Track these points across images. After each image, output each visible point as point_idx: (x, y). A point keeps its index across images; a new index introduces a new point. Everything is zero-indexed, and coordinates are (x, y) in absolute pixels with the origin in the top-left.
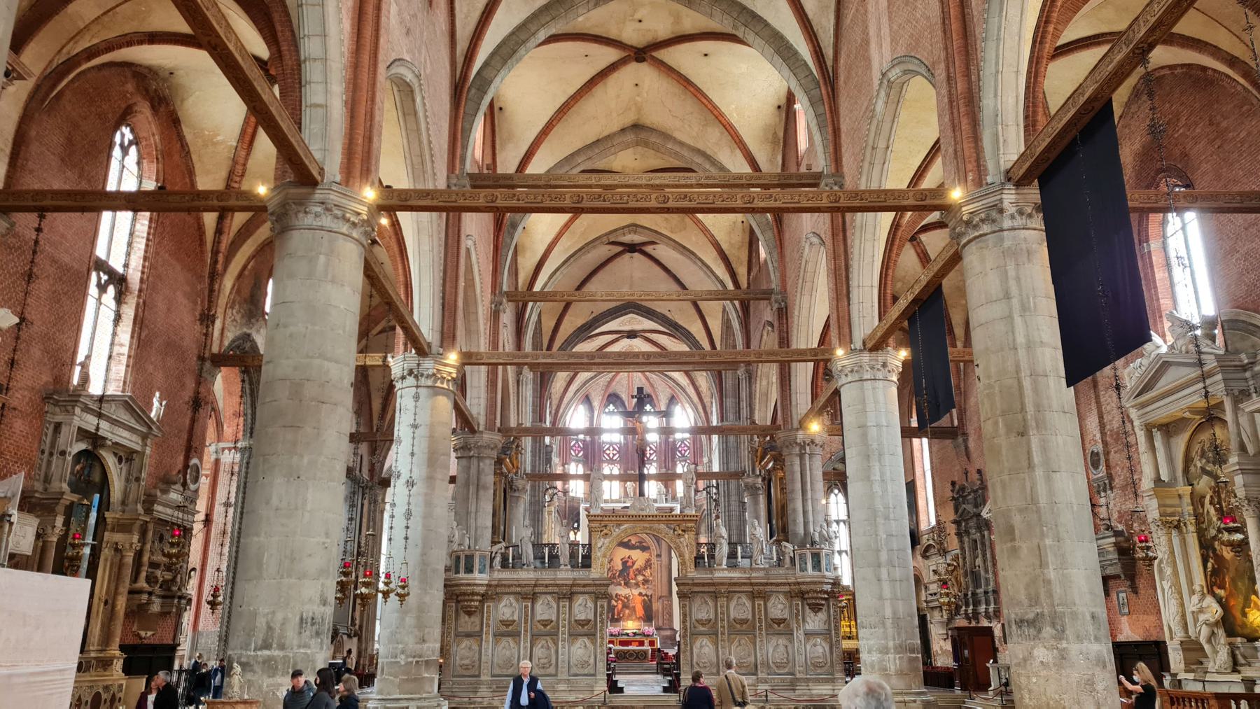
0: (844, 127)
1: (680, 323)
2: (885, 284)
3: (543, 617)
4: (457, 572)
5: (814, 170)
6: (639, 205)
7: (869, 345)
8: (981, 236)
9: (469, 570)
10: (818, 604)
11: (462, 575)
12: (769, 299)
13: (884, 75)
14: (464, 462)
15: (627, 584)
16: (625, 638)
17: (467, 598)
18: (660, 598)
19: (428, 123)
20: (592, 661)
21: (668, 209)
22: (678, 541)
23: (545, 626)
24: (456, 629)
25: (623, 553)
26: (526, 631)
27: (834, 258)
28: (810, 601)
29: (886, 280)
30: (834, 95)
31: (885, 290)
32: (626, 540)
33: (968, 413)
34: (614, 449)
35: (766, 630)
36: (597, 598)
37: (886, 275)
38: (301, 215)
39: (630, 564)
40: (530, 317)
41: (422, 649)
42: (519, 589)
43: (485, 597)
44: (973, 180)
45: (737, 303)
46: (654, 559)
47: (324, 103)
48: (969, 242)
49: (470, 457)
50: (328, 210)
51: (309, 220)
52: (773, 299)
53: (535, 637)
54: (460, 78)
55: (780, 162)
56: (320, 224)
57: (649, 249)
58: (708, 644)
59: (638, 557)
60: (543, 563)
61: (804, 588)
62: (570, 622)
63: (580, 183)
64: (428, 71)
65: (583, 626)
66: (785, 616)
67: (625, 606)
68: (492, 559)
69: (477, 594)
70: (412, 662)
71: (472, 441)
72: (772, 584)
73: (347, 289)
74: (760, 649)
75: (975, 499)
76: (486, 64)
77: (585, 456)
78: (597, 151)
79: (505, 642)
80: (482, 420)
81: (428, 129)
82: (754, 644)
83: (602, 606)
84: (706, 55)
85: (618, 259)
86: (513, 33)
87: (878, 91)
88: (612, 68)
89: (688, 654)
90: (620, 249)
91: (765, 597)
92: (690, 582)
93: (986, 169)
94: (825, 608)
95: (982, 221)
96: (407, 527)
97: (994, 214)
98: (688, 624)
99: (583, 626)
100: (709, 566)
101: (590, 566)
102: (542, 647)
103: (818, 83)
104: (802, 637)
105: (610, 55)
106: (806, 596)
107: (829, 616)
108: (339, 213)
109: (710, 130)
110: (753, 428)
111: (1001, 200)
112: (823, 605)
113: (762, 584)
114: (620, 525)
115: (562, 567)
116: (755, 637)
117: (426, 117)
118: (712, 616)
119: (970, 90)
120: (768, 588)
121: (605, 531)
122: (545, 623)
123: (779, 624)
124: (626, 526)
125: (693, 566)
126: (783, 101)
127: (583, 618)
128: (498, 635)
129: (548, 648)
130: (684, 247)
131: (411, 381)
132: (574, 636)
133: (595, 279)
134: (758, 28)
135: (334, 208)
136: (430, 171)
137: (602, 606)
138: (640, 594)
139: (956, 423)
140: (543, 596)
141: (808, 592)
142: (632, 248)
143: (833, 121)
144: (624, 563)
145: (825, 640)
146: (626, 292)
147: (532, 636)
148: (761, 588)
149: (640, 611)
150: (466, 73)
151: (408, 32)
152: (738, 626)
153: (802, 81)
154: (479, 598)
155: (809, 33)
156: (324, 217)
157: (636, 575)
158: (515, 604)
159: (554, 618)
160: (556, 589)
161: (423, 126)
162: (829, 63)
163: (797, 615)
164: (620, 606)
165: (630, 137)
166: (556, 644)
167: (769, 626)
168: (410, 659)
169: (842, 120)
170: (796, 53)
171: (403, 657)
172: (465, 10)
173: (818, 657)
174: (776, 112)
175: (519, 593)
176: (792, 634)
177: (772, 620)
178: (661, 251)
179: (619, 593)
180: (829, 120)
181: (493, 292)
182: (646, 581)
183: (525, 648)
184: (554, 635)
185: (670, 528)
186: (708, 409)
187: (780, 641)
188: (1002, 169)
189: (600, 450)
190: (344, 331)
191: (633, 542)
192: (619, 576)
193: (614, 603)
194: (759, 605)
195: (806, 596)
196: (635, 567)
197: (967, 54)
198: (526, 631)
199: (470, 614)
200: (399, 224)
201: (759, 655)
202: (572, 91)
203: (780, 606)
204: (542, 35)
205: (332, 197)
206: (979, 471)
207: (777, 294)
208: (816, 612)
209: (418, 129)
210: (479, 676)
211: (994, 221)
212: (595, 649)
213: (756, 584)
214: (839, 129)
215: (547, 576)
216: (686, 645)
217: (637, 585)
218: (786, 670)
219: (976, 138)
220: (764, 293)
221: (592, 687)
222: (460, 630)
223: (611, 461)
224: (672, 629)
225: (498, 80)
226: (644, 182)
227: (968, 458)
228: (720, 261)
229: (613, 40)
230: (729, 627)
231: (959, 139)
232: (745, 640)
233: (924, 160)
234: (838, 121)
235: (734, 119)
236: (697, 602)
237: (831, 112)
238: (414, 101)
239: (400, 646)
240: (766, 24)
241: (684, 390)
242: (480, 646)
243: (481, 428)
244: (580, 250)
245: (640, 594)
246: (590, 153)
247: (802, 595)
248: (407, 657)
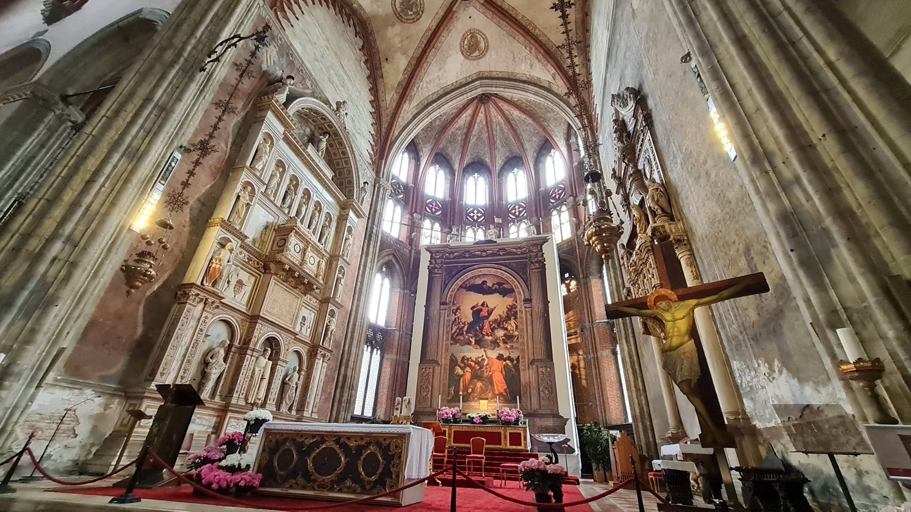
15: (479, 343)
16: (465, 427)
18: (532, 363)
25: (476, 299)
32: (479, 281)
34: (479, 212)
39: (484, 313)
46: (520, 306)
59: (497, 304)
67: (476, 376)
77: (444, 214)
144: (476, 312)
149: (500, 384)
157: (493, 329)
164: (468, 376)
179: (468, 355)
182: (509, 338)
189: (461, 213)
191: (490, 284)
192: (468, 331)
196: (491, 318)
217: (495, 344)
224: (556, 415)
245: (500, 357)
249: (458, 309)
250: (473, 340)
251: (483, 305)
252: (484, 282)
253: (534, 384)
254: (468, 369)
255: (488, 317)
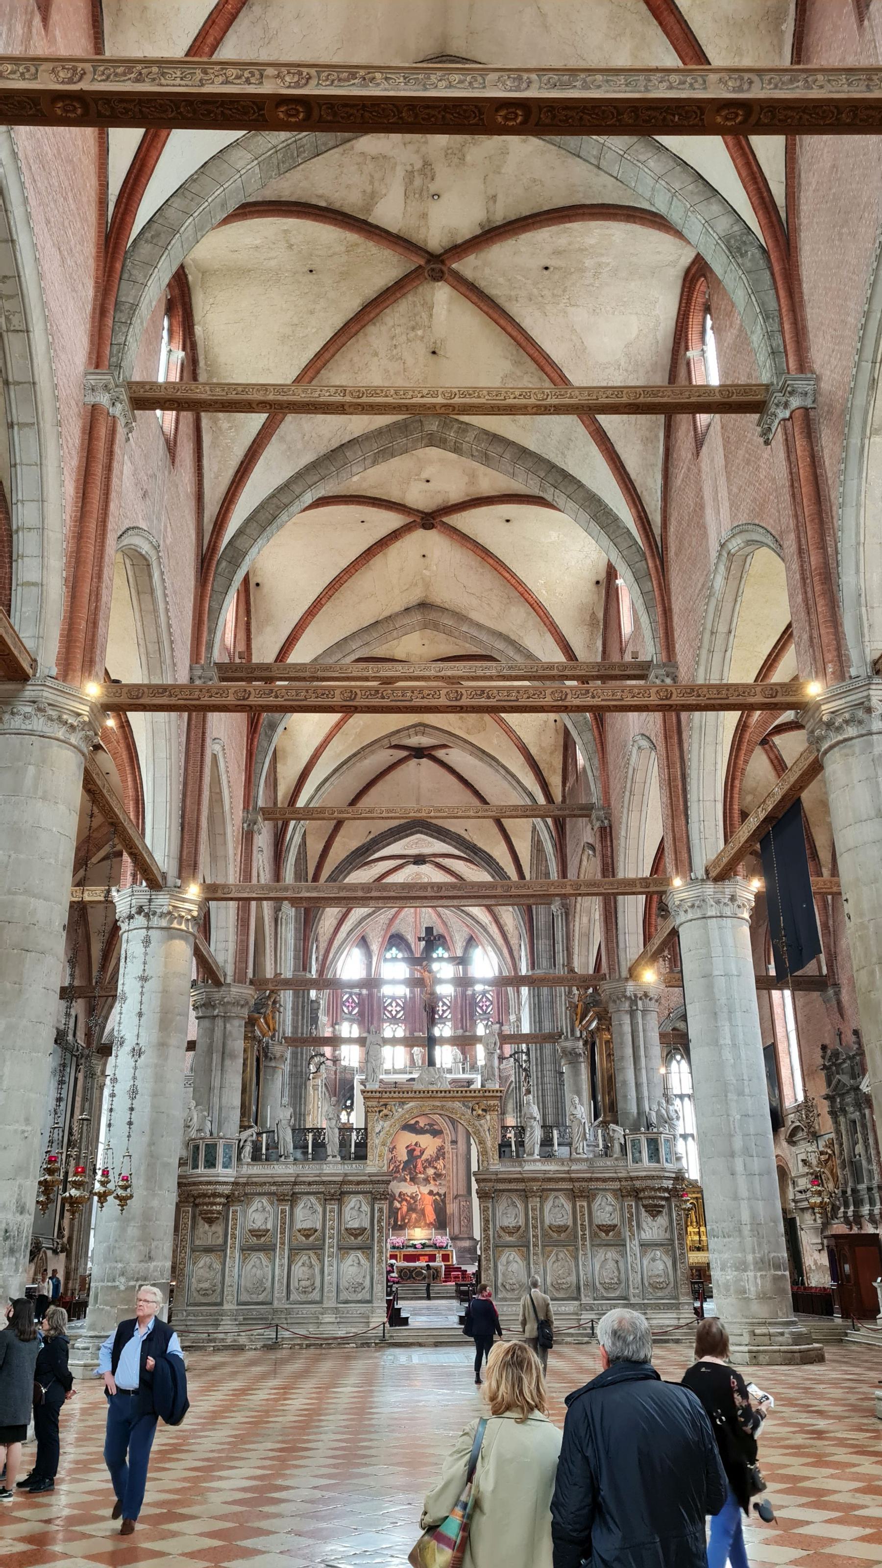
0: (677, 605)
1: (480, 845)
2: (732, 797)
3: (307, 1225)
4: (195, 1166)
5: (642, 658)
6: (425, 702)
7: (713, 874)
8: (846, 740)
9: (211, 1163)
10: (656, 1206)
11: (201, 1170)
12: (589, 816)
13: (722, 546)
14: (206, 1023)
15: (413, 1180)
16: (411, 1251)
17: (207, 1200)
18: (456, 1198)
19: (167, 603)
20: (367, 1283)
21: (461, 707)
22: (477, 1123)
23: (307, 1236)
24: (192, 1241)
25: (409, 1138)
26: (283, 1244)
27: (668, 766)
28: (646, 1202)
29: (732, 793)
30: (663, 569)
31: (731, 805)
32: (413, 1122)
33: (839, 958)
34: (398, 1005)
35: (591, 1240)
36: (375, 1199)
37: (732, 786)
38: (6, 717)
39: (417, 1153)
40: (292, 838)
41: (147, 1269)
42: (274, 1188)
43: (230, 1199)
44: (833, 673)
45: (549, 821)
46: (448, 1147)
47: (39, 581)
48: (832, 747)
49: (214, 1017)
50: (39, 710)
51: (17, 723)
52: (593, 816)
53: (295, 1251)
54: (208, 548)
55: (600, 649)
56: (30, 727)
57: (440, 754)
58: (518, 1259)
59: (428, 1144)
60: (305, 1153)
61: (638, 1184)
62: (339, 1231)
63: (354, 674)
64: (168, 541)
65: (356, 1236)
66: (615, 1222)
67: (411, 1209)
68: (240, 1149)
69: (220, 1195)
70: (134, 1287)
71: (217, 996)
72: (598, 1179)
73: (62, 808)
74: (584, 1265)
75: (852, 1068)
76: (240, 532)
77: (361, 1014)
78: (375, 635)
79: (256, 1258)
80: (230, 970)
81: (167, 610)
82: (576, 1258)
83: (381, 1210)
84: (508, 521)
85: (403, 767)
86: (272, 496)
87: (716, 565)
88: (395, 536)
89: (491, 1272)
90: (404, 753)
91: (589, 1196)
92: (493, 1177)
93: (849, 659)
94: (665, 1210)
95: (846, 722)
96: (132, 1109)
97: (860, 714)
98: (491, 1233)
99: (356, 1236)
100: (518, 1156)
101: (365, 1157)
102: (303, 1265)
103: (644, 553)
104: (637, 1249)
105: (392, 521)
106: (641, 1195)
107: (671, 1221)
108: (54, 714)
109: (513, 609)
110: (572, 979)
111: (868, 697)
112: (663, 1206)
113: (584, 1180)
114: (403, 1103)
115: (330, 1158)
116: (577, 1249)
117: (165, 595)
118: (521, 1222)
119: (826, 565)
120: (593, 1185)
121: (385, 1112)
122: (308, 1233)
123: (607, 1232)
124: (411, 1104)
125: (496, 1157)
126: (602, 576)
127: (356, 1226)
128: (247, 1250)
129: (311, 1266)
130: (484, 752)
131: (140, 920)
132: (345, 1249)
133: (373, 791)
134: (570, 489)
135: (48, 708)
136: (168, 661)
137: (381, 1210)
138: (431, 1193)
139: (825, 971)
140: (305, 1197)
141: (643, 1190)
142: (419, 753)
143: (663, 600)
144: (410, 1152)
145: (667, 1252)
146: (411, 807)
147: (290, 1250)
148: (584, 1184)
149: (431, 1216)
150: (215, 542)
151: (144, 496)
152: (555, 1235)
153: (625, 553)
154: (223, 1200)
155: (631, 495)
156: (35, 719)
157: (425, 1168)
158: (269, 1208)
159: (319, 1226)
160: (322, 1188)
161: (161, 606)
162: (657, 531)
163: (630, 1220)
164: (405, 1209)
165: (416, 618)
166: (322, 1261)
167: (594, 1236)
168: (132, 1283)
169: (673, 599)
170: (616, 519)
171: (123, 1280)
172: (216, 469)
173: (658, 1276)
174: (594, 588)
175: (274, 1194)
176: (625, 1245)
177: (598, 1226)
178: (456, 757)
179: (404, 1191)
180: (658, 599)
181: (246, 808)
182: (438, 1176)
183: (282, 1265)
184: (318, 1248)
185: (467, 1107)
186: (515, 953)
187: (609, 1255)
188: (869, 660)
189: (379, 1007)
190: (56, 860)
191: (422, 1124)
192: (404, 1169)
193: (397, 1204)
194: (582, 1207)
195: (641, 1195)
196: (424, 1157)
197: (821, 522)
198: (283, 1244)
199: (210, 1221)
200: (129, 725)
201: (581, 1273)
202: (344, 563)
203: (609, 1209)
204: (308, 498)
205: (45, 694)
206: (856, 1033)
207: (599, 809)
208: (654, 1216)
209: (155, 611)
210: (221, 1304)
211: (860, 722)
212: (372, 1267)
213: (578, 1180)
214: (670, 609)
215: (310, 1170)
216: (488, 1260)
217: (427, 1180)
218: (617, 1294)
219: (835, 622)
220: (581, 809)
221: (368, 1317)
222: (197, 1243)
223: (394, 1020)
224: (472, 1239)
225: (254, 551)
226: (432, 673)
227: (842, 1015)
228: (528, 769)
229: (395, 503)
230: (543, 1236)
231: (814, 623)
232: (564, 1254)
233: (775, 647)
234: (669, 599)
235: (542, 595)
236: (502, 1205)
237: (661, 590)
238: (150, 576)
239: (120, 1265)
240: (580, 485)
241: (485, 930)
242: (224, 1264)
243: (229, 980)
244: (354, 755)
245: (431, 1193)
246: (366, 638)
247: (636, 1194)
248: (129, 1280)
249: (394, 1147)
250: (408, 1177)
251: (416, 1144)
252: (417, 1122)
253: (456, 1214)
254: (404, 1203)
255: (420, 1157)
